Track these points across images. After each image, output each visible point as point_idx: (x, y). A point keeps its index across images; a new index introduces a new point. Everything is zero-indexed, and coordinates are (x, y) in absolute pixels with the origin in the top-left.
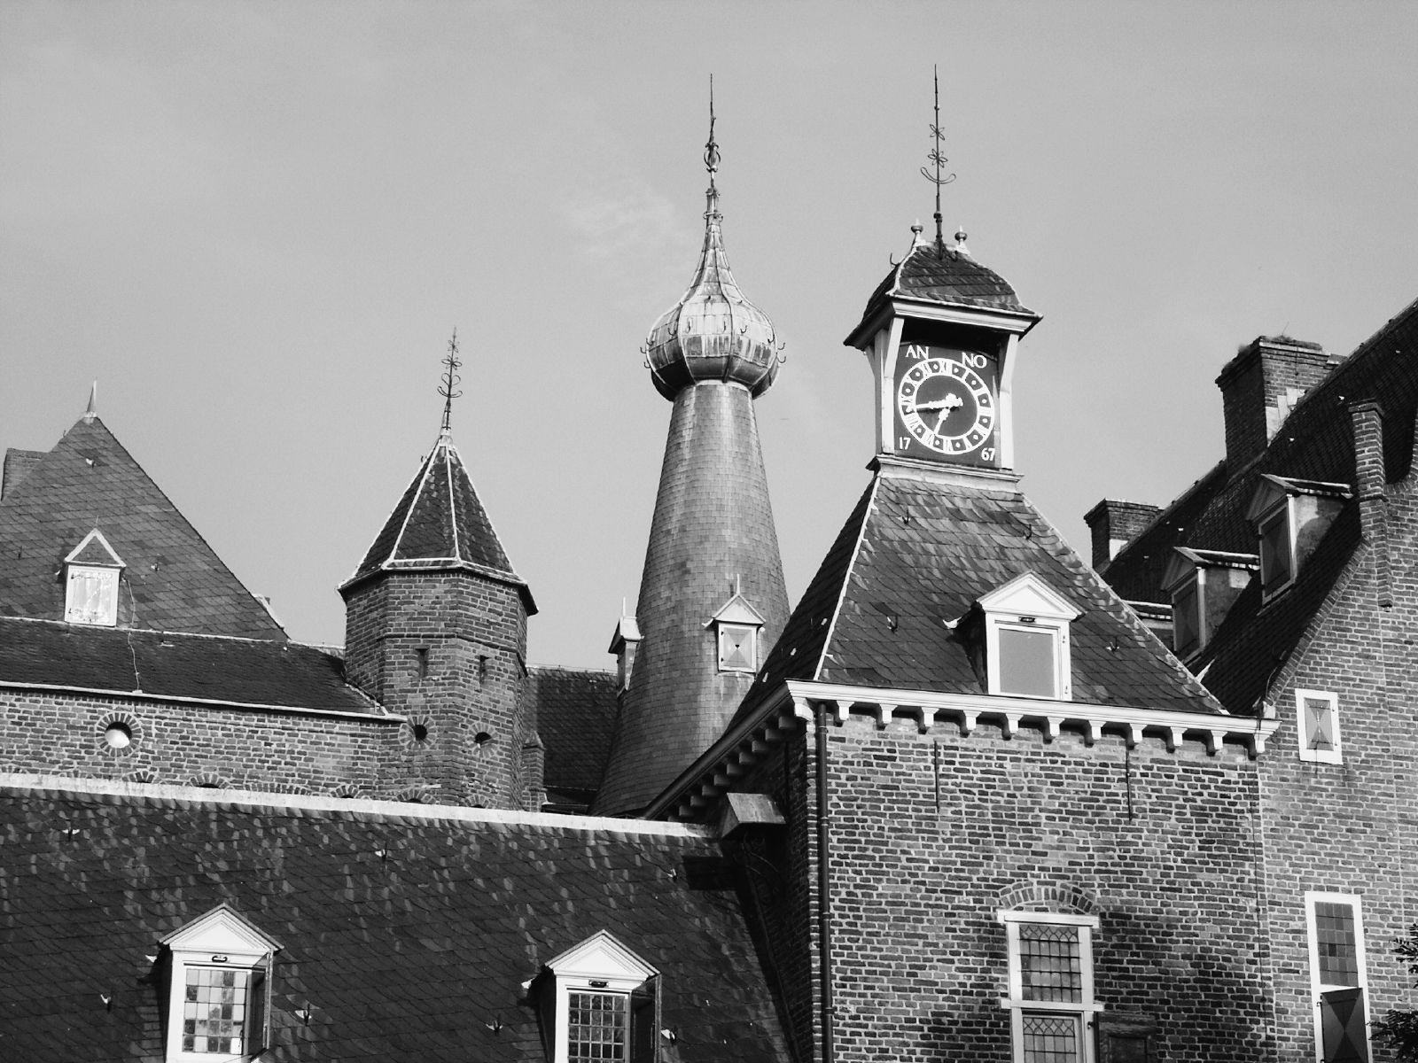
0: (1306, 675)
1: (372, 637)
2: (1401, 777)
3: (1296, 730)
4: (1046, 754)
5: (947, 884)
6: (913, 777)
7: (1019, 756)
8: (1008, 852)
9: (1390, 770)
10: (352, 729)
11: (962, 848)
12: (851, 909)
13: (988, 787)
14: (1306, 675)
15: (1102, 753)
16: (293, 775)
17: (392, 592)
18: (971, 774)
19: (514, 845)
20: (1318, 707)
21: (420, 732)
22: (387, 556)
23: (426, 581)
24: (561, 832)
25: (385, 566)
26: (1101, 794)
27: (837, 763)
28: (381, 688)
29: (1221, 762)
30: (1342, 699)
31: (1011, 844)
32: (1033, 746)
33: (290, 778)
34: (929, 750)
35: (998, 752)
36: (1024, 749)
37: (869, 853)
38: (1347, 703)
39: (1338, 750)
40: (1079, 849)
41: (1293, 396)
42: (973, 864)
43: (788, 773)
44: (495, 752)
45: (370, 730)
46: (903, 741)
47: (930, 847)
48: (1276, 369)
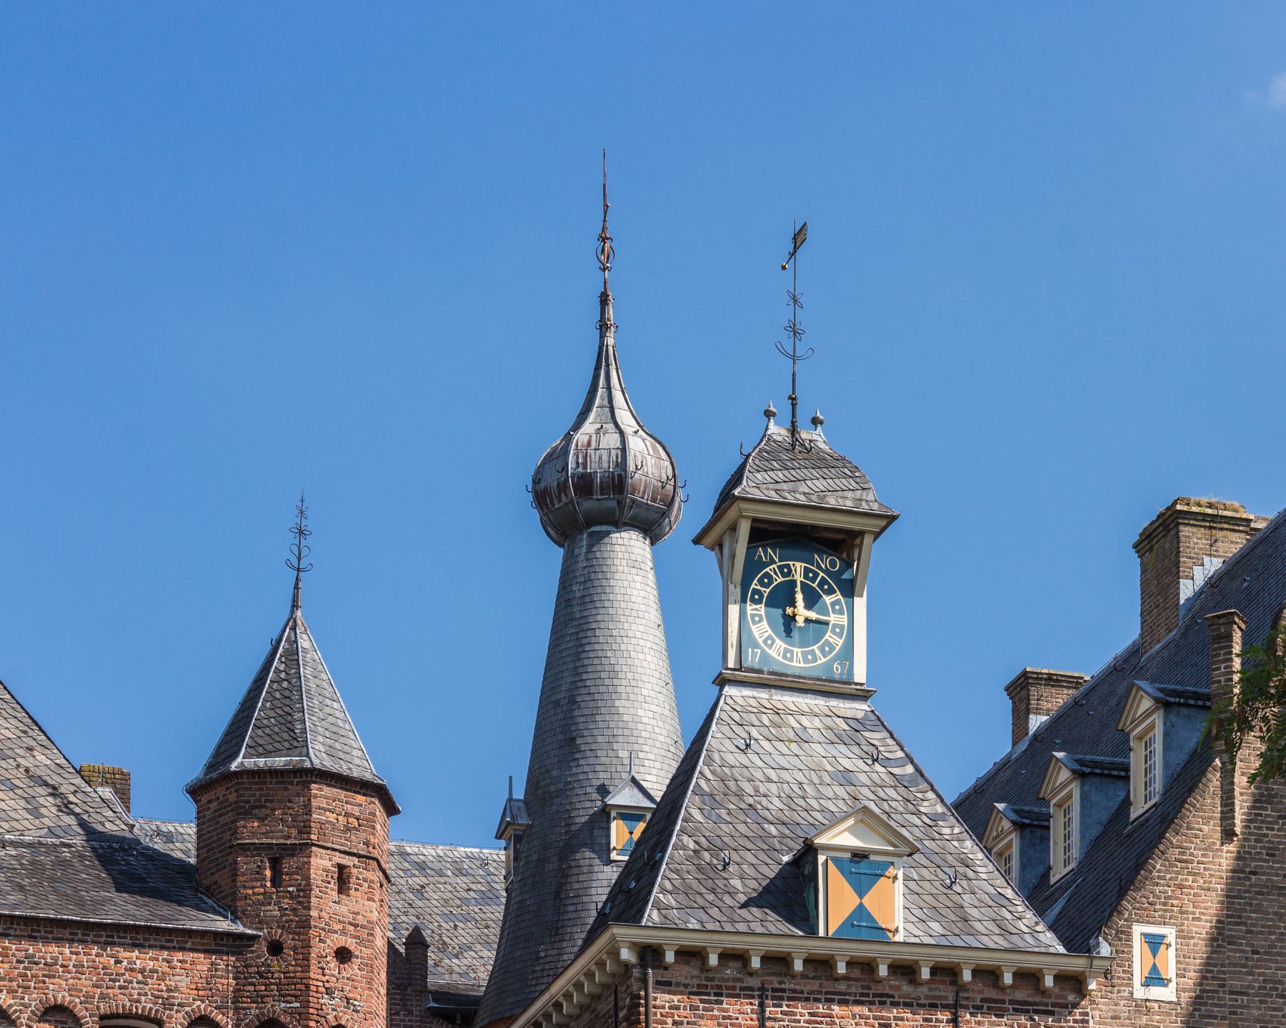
0: (1145, 909)
1: (223, 844)
3: (1130, 966)
4: (874, 995)
6: (740, 1020)
7: (847, 997)
10: (206, 944)
14: (1145, 909)
15: (931, 993)
16: (146, 994)
17: (243, 795)
18: (798, 1017)
20: (1155, 943)
21: (276, 948)
22: (236, 755)
23: (277, 783)
27: (663, 1007)
28: (234, 900)
29: (1053, 1000)
32: (863, 987)
33: (143, 998)
34: (756, 993)
35: (826, 993)
36: (853, 990)
38: (1184, 937)
39: (1173, 986)
41: (1213, 565)
43: (617, 1016)
44: (356, 967)
45: (223, 945)
46: (730, 984)
48: (1193, 537)
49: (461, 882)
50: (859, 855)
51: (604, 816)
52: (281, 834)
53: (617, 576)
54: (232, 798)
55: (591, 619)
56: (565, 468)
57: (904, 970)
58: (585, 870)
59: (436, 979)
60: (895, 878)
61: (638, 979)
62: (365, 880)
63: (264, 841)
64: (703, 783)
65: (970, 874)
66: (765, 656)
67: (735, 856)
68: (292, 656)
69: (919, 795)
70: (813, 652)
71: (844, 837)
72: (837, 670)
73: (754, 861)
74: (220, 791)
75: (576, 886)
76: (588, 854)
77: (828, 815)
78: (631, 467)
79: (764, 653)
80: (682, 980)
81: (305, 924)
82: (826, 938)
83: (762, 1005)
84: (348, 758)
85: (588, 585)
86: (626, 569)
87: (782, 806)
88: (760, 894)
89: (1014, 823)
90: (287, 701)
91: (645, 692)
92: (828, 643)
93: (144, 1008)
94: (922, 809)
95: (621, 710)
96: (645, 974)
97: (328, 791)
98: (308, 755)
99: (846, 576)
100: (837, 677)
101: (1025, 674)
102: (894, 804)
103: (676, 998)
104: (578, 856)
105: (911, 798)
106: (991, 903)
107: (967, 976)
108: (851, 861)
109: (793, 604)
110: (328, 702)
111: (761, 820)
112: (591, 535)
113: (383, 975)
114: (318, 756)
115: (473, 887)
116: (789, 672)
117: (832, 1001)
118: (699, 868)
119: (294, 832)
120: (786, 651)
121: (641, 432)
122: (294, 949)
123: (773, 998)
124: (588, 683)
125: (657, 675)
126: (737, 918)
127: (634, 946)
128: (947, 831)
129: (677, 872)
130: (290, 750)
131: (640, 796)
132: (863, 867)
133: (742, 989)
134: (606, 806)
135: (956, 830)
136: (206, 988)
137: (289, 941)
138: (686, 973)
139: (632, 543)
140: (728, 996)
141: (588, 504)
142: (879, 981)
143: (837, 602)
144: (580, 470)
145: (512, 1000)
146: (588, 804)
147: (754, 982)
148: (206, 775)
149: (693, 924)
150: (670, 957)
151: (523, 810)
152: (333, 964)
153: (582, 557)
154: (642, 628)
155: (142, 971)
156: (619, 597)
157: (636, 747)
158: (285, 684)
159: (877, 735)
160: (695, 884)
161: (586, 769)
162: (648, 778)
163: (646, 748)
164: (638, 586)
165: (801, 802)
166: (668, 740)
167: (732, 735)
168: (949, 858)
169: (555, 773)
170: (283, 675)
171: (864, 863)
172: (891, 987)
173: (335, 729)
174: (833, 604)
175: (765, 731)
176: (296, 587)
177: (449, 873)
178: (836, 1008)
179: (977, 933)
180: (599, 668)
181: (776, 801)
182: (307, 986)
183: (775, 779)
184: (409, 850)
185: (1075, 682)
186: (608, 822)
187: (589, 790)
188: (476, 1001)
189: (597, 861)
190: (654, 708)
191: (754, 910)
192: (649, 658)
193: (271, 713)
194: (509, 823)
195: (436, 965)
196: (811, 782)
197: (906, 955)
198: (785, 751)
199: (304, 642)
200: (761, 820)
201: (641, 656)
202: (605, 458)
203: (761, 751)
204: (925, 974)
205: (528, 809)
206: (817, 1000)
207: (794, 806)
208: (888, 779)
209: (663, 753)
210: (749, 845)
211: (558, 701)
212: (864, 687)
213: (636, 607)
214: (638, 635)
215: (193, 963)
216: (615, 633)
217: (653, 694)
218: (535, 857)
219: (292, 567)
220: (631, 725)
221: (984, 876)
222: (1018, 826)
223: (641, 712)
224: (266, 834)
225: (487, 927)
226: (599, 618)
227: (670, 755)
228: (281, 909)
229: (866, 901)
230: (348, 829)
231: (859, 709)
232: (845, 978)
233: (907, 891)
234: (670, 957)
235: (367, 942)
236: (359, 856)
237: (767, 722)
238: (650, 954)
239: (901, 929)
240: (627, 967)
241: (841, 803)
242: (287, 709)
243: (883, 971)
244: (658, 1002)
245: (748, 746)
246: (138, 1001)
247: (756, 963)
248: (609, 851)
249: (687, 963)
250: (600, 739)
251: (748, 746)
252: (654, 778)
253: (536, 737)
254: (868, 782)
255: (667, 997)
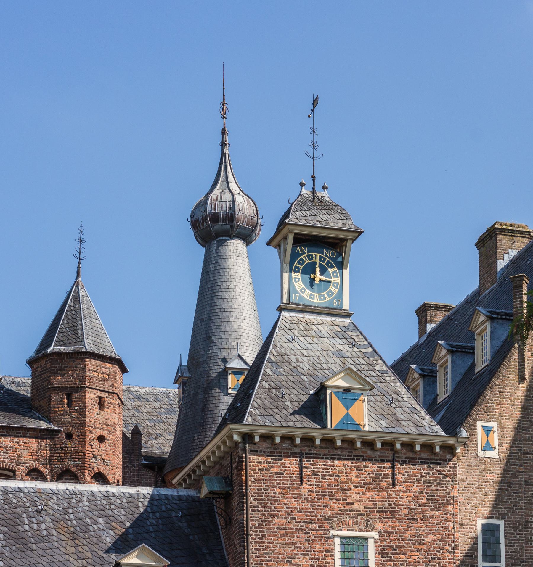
0: (483, 415)
1: (44, 387)
2: (527, 463)
3: (476, 441)
4: (354, 456)
5: (306, 519)
6: (291, 468)
7: (342, 457)
8: (335, 503)
9: (521, 460)
10: (36, 434)
11: (313, 502)
12: (260, 532)
13: (326, 472)
14: (483, 415)
15: (381, 455)
16: (7, 458)
17: (53, 364)
18: (318, 467)
19: (105, 502)
20: (488, 430)
21: (69, 436)
23: (70, 358)
24: (127, 495)
25: (49, 351)
26: (381, 475)
27: (254, 462)
28: (50, 413)
29: (439, 457)
30: (500, 426)
31: (337, 500)
32: (349, 452)
33: (6, 460)
34: (298, 455)
35: (332, 455)
36: (344, 453)
37: (269, 505)
38: (502, 428)
39: (496, 450)
40: (369, 501)
41: (513, 253)
42: (318, 509)
43: (232, 466)
44: (107, 445)
45: (44, 435)
46: (286, 451)
47: (297, 501)
48: (503, 240)
49: (157, 404)
50: (346, 390)
51: (225, 372)
52: (71, 382)
53: (231, 260)
54: (48, 365)
55: (218, 281)
56: (206, 210)
57: (369, 444)
58: (216, 398)
59: (146, 450)
60: (364, 401)
61: (242, 449)
62: (112, 404)
63: (64, 385)
64: (272, 357)
65: (399, 398)
66: (301, 297)
67: (287, 391)
68: (77, 299)
69: (375, 362)
70: (324, 295)
71: (339, 382)
72: (335, 304)
73: (297, 393)
74: (43, 363)
75: (212, 405)
76: (217, 391)
77: (331, 371)
78: (237, 210)
79: (300, 296)
80: (263, 449)
81: (83, 424)
82: (331, 429)
83: (301, 461)
84: (103, 346)
85: (217, 265)
86: (235, 257)
87: (309, 367)
88: (300, 409)
89: (420, 374)
90: (74, 320)
91: (244, 314)
92: (331, 291)
93: (6, 465)
94: (376, 368)
95: (233, 323)
96: (245, 447)
97: (94, 362)
98: (84, 345)
99: (339, 260)
100: (335, 307)
101: (424, 305)
102: (363, 366)
103: (260, 458)
104: (213, 391)
105: (371, 363)
106: (409, 412)
107: (398, 446)
108: (343, 393)
109: (314, 273)
110: (94, 320)
111: (300, 374)
112: (218, 241)
113: (121, 448)
114: (89, 345)
115: (163, 406)
116: (313, 305)
117: (334, 459)
118: (270, 397)
119: (78, 381)
120: (311, 295)
121: (241, 193)
122: (78, 436)
123: (306, 457)
124: (217, 311)
125: (250, 306)
126: (288, 420)
127: (240, 433)
128: (388, 378)
129: (260, 398)
130: (75, 343)
131: (242, 363)
132: (348, 396)
133: (291, 453)
134: (226, 368)
135: (393, 378)
136: (37, 455)
137: (75, 433)
138: (265, 446)
139: (238, 245)
140: (285, 457)
141: (216, 227)
142: (357, 449)
143: (335, 272)
144: (213, 211)
145: (182, 459)
146: (217, 367)
147: (297, 450)
148: (36, 355)
149: (268, 423)
150: (257, 439)
151: (187, 370)
152: (97, 443)
153: (214, 252)
154: (242, 285)
155: (6, 447)
156: (232, 270)
157: (240, 340)
158: (73, 312)
159: (354, 334)
160: (268, 404)
161: (216, 351)
162: (246, 354)
163: (245, 341)
164: (241, 265)
165: (319, 366)
166: (256, 337)
167: (286, 334)
168: (389, 391)
169: (201, 353)
170: (72, 308)
171: (349, 394)
172: (362, 452)
173: (97, 333)
174: (333, 273)
175: (301, 333)
176: (79, 267)
177: (152, 400)
178: (336, 462)
179: (402, 426)
180: (222, 303)
181: (307, 365)
182: (84, 454)
183: (306, 354)
184: (132, 389)
185: (448, 308)
186: (227, 375)
187: (218, 360)
188: (165, 460)
189: (222, 394)
190: (248, 322)
191: (297, 416)
192: (246, 299)
193: (67, 326)
194: (180, 377)
195: (146, 443)
196: (324, 356)
197: (369, 437)
198: (311, 341)
199: (82, 292)
200: (300, 374)
201: (242, 298)
202: (224, 206)
203: (299, 342)
204: (378, 445)
205: (189, 370)
206: (327, 458)
207: (315, 367)
208: (360, 355)
209: (253, 343)
210: (294, 386)
211: (203, 319)
212: (349, 311)
213: (240, 275)
214: (241, 288)
215: (30, 443)
216: (230, 287)
217: (248, 315)
218: (192, 392)
219: (76, 257)
220: (238, 330)
221: (406, 399)
222: (422, 376)
223: (242, 324)
224: (64, 383)
225: (170, 425)
226: (222, 280)
227: (256, 344)
228: (72, 418)
229: (350, 411)
230: (103, 380)
231: (346, 321)
232: (340, 448)
233: (369, 407)
234: (257, 439)
235: (112, 432)
236: (109, 392)
237: (302, 328)
238: (247, 437)
239: (367, 425)
240: (236, 443)
241: (337, 366)
242: (75, 324)
243: (358, 444)
244: (251, 460)
245: (293, 339)
246: (4, 461)
247: (298, 441)
248: (227, 389)
249: (265, 441)
250: (223, 337)
251: (293, 339)
252: (248, 355)
253: (192, 336)
254: (351, 356)
255: (256, 457)
